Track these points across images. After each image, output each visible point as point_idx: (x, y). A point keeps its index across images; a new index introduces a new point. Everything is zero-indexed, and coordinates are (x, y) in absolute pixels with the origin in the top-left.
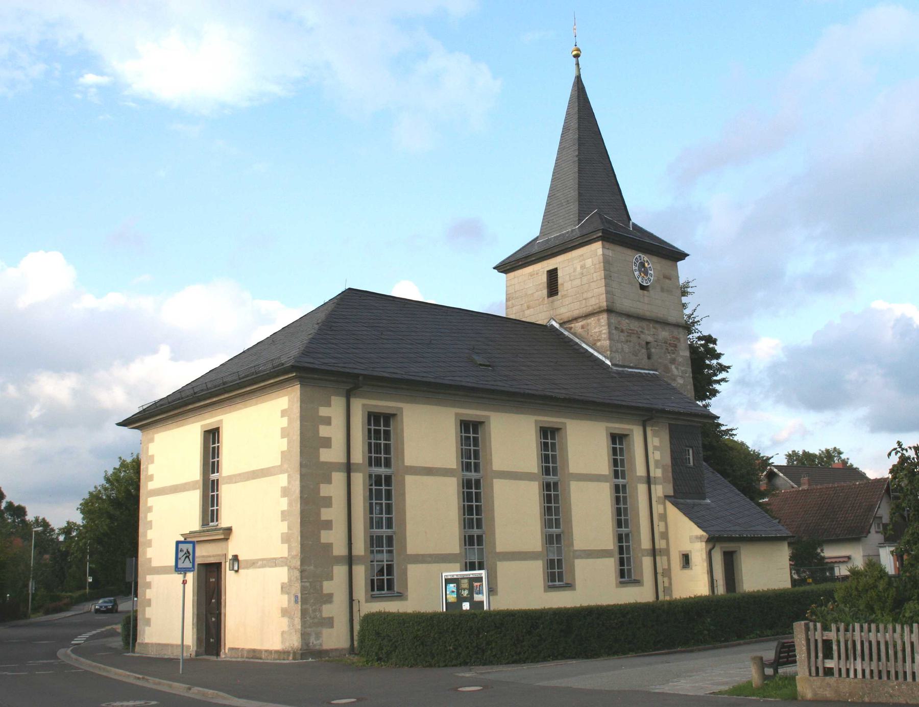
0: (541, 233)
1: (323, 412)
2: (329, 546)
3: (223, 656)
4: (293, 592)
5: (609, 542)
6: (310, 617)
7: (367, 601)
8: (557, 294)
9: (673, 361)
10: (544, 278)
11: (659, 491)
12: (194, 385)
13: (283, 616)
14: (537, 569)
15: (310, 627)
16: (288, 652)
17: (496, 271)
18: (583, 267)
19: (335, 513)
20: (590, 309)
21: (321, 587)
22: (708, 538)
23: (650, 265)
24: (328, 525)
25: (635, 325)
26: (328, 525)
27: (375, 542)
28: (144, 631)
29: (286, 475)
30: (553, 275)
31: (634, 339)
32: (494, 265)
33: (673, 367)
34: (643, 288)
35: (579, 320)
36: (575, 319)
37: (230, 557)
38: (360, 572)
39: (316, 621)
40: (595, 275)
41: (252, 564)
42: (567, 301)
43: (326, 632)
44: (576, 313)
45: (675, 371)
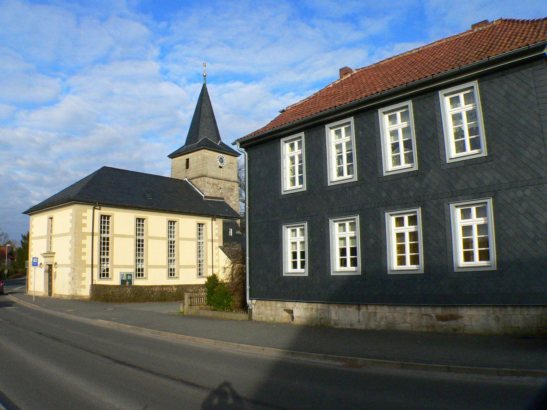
0: (186, 143)
1: (84, 214)
2: (85, 261)
3: (52, 296)
4: (72, 276)
5: (194, 263)
6: (77, 285)
7: (98, 280)
8: (188, 168)
9: (231, 195)
10: (185, 162)
11: (216, 244)
12: (45, 201)
13: (69, 284)
14: (165, 272)
15: (77, 288)
16: (70, 296)
17: (168, 157)
18: (197, 159)
19: (87, 250)
20: (199, 175)
21: (81, 274)
22: (232, 262)
23: (225, 159)
24: (84, 254)
25: (215, 181)
26: (84, 254)
27: (102, 261)
28: (30, 286)
29: (71, 236)
30: (188, 160)
31: (215, 186)
32: (167, 155)
33: (231, 197)
34: (220, 167)
35: (195, 179)
36: (193, 178)
37: (55, 263)
38: (96, 271)
39: (79, 286)
40: (201, 162)
41: (61, 266)
42: (191, 171)
43: (83, 289)
44: (194, 176)
45: (232, 199)
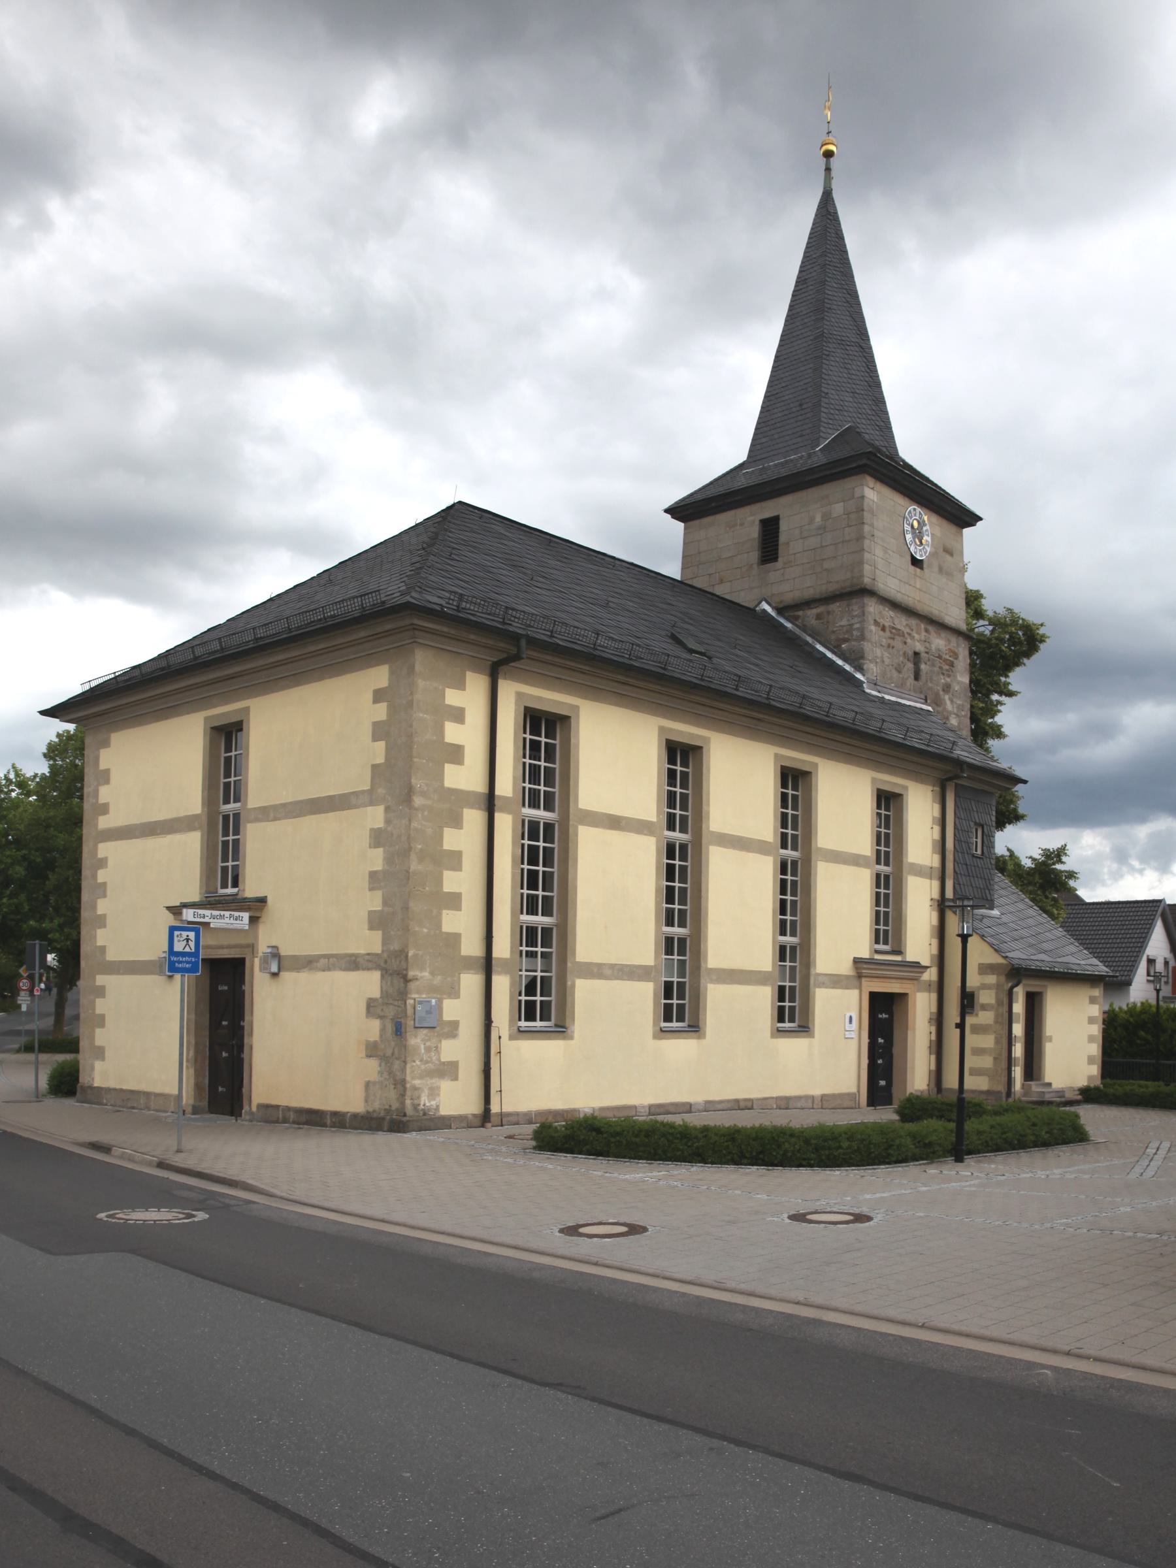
0: (749, 456)
1: (453, 697)
7: (511, 1038)
9: (947, 688)
15: (421, 1077)
17: (669, 516)
20: (833, 588)
25: (902, 622)
26: (454, 900)
30: (770, 528)
32: (666, 506)
33: (947, 697)
34: (916, 562)
38: (502, 985)
41: (307, 963)
43: (445, 1085)
44: (808, 594)
